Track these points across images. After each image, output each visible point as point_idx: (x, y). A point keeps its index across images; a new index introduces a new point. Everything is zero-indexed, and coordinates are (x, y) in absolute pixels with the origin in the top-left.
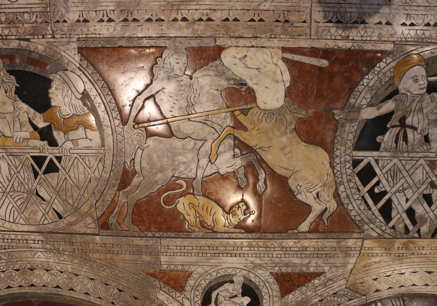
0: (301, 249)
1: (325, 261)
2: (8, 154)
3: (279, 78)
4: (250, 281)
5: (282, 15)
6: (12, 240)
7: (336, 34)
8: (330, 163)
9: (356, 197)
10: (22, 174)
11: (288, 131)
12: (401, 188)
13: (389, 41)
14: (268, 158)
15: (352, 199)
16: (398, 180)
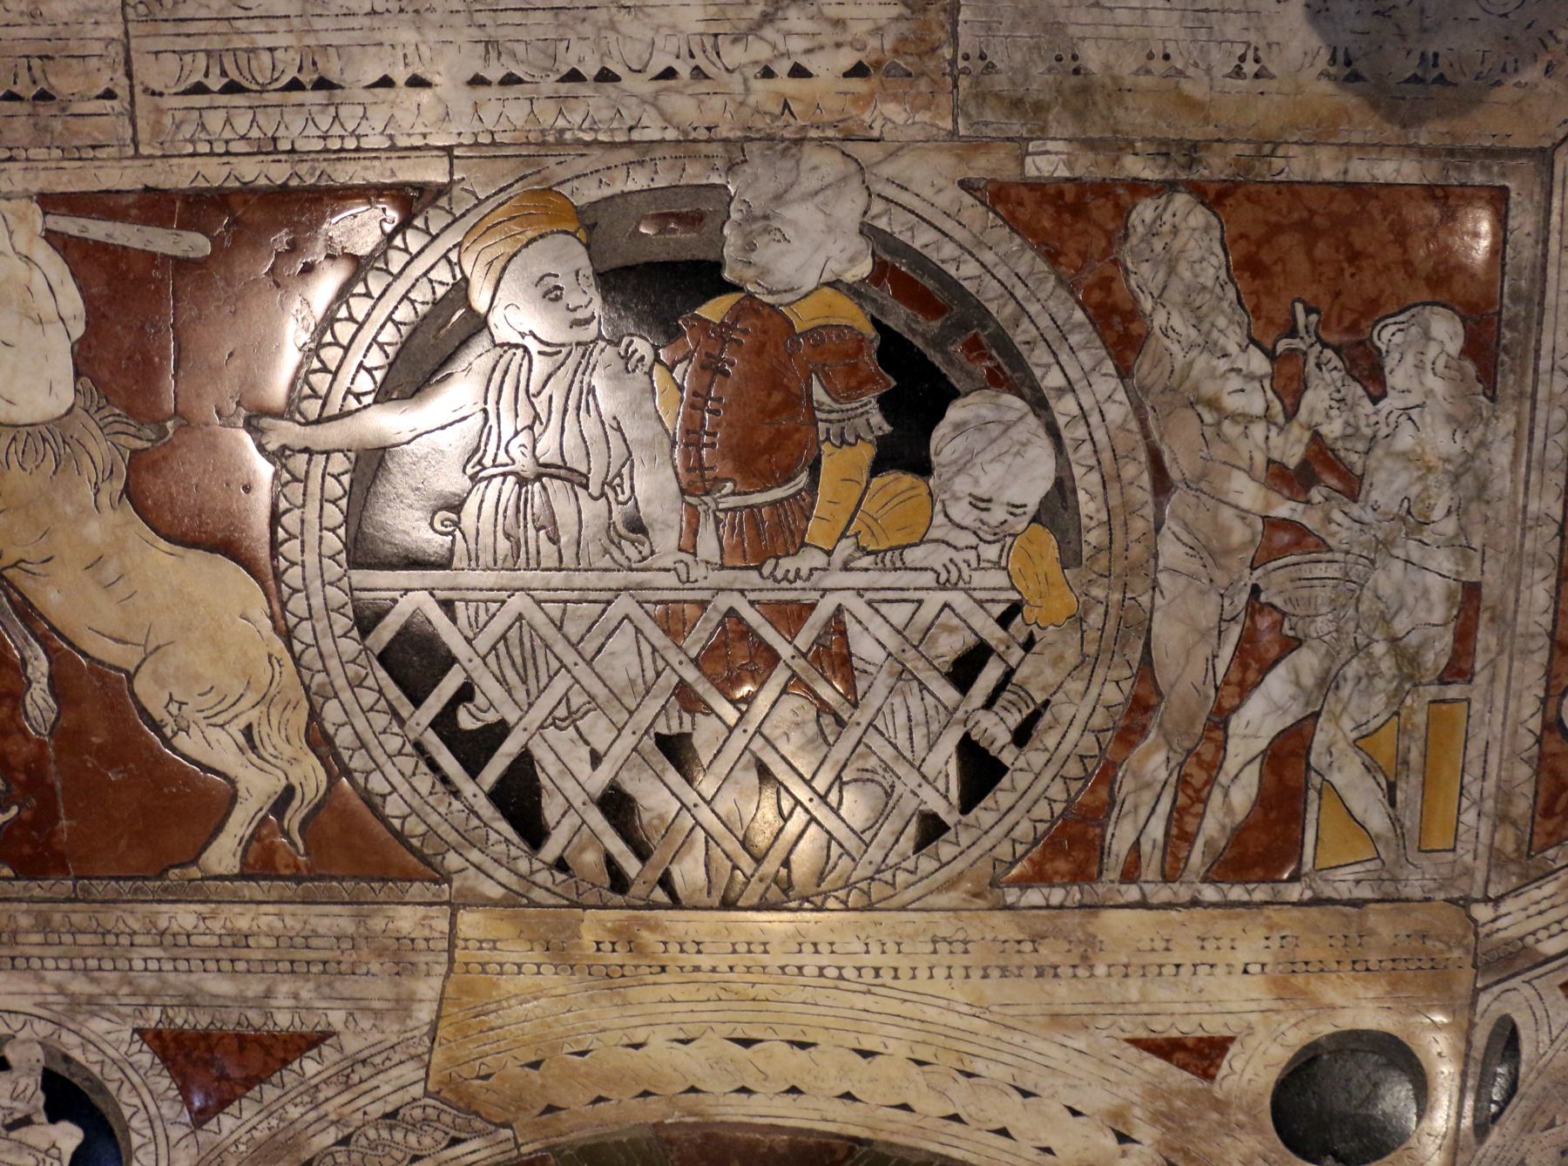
0: (228, 941)
1: (326, 991)
3: (46, 306)
4: (67, 1059)
5: (24, 77)
7: (227, 134)
8: (272, 617)
9: (394, 743)
11: (104, 499)
12: (562, 712)
13: (427, 147)
14: (51, 599)
15: (378, 753)
16: (544, 680)
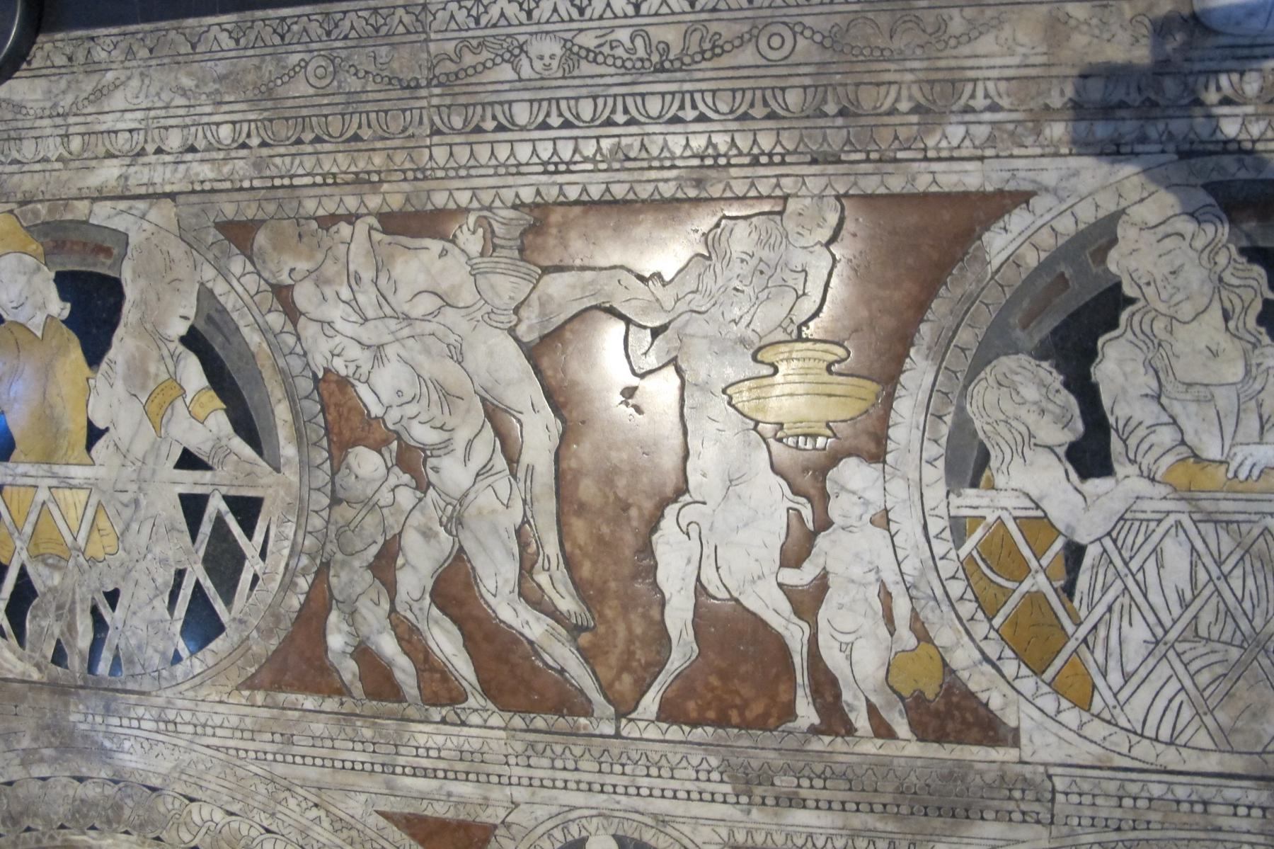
2: (1196, 517)
6: (1150, 800)
10: (1236, 583)
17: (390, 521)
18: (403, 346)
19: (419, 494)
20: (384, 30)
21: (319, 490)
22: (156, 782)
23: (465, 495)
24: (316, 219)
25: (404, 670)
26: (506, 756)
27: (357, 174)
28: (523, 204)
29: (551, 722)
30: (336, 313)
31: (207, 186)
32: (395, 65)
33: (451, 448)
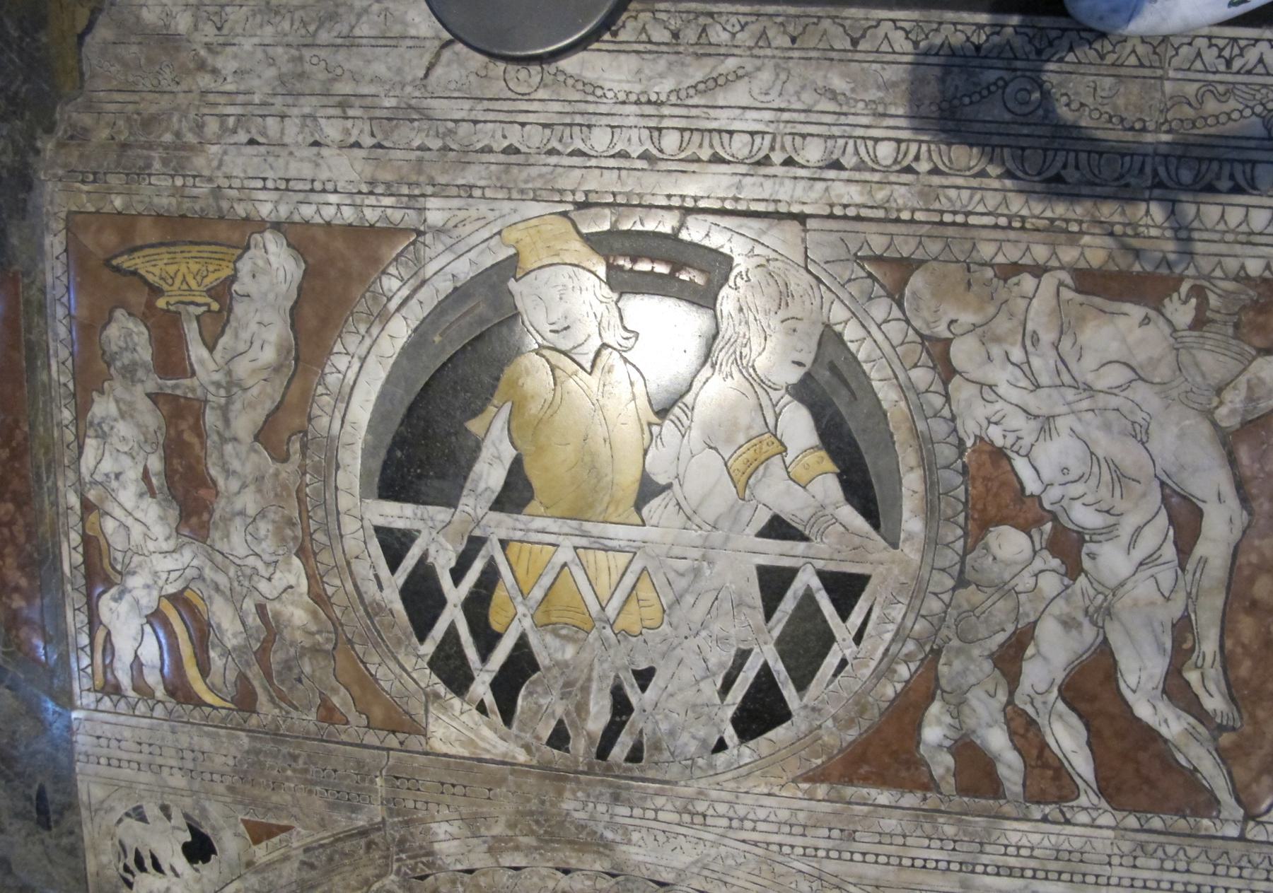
17: (1026, 607)
18: (1080, 420)
19: (1066, 581)
20: (1110, 59)
21: (944, 570)
22: (667, 877)
23: (1122, 584)
24: (992, 266)
25: (1010, 765)
26: (1109, 856)
27: (1052, 220)
28: (1248, 277)
29: (1169, 822)
30: (1001, 376)
31: (851, 212)
32: (1120, 102)
33: (1116, 533)
